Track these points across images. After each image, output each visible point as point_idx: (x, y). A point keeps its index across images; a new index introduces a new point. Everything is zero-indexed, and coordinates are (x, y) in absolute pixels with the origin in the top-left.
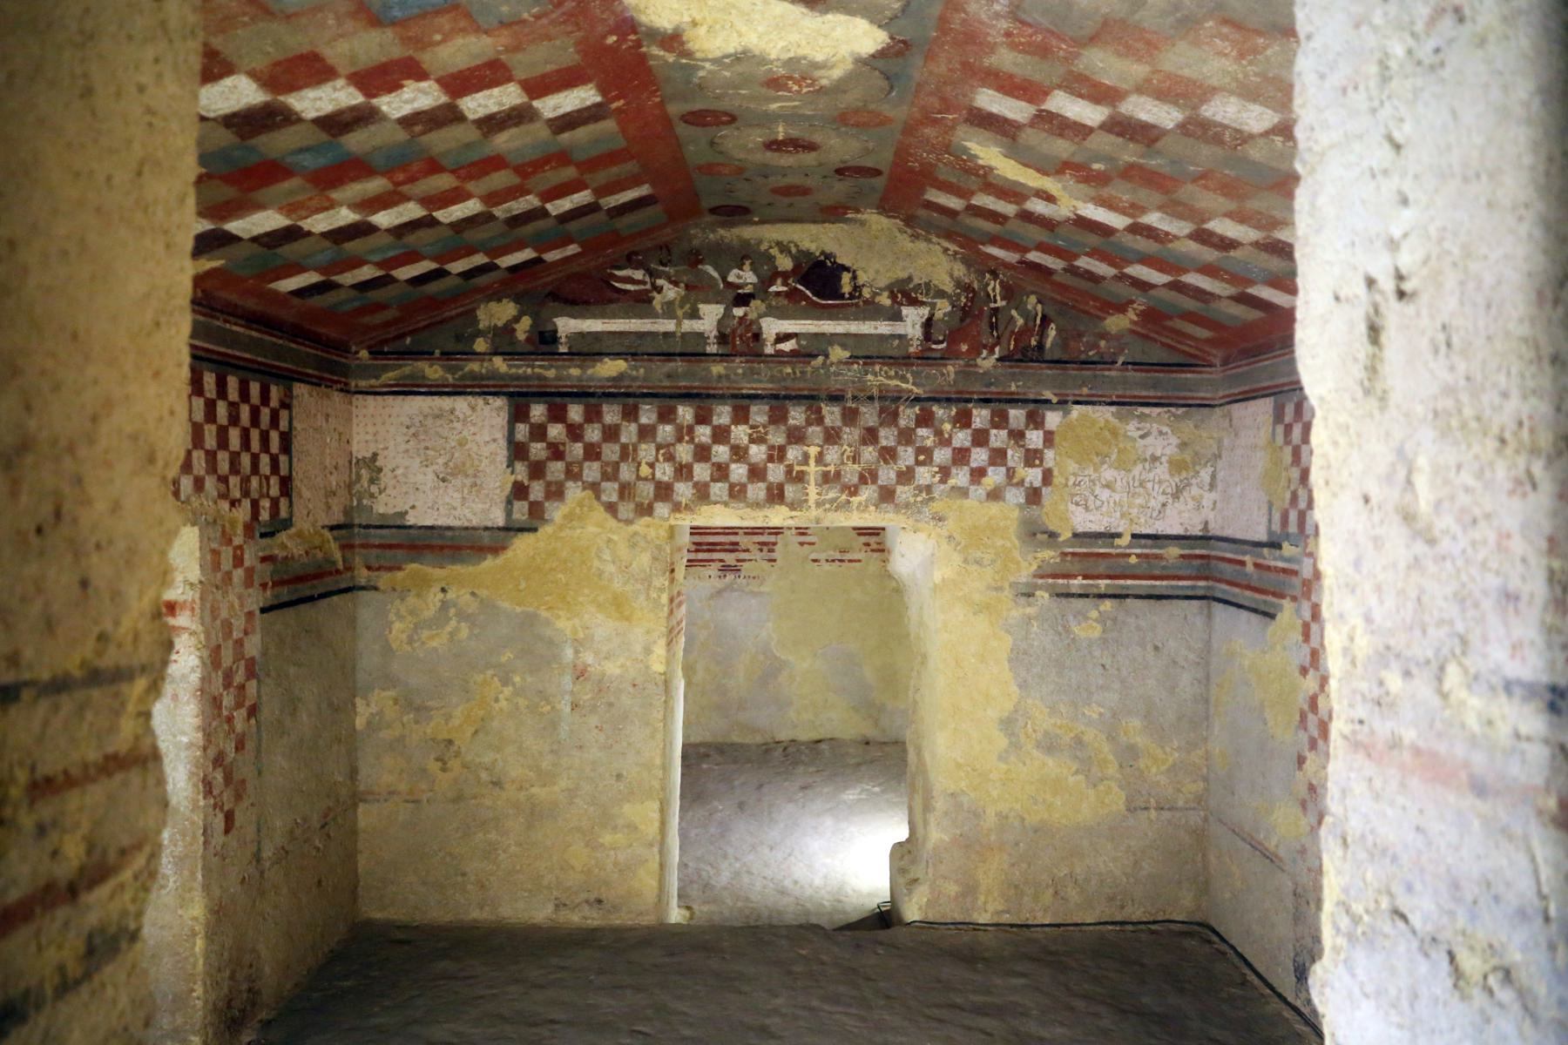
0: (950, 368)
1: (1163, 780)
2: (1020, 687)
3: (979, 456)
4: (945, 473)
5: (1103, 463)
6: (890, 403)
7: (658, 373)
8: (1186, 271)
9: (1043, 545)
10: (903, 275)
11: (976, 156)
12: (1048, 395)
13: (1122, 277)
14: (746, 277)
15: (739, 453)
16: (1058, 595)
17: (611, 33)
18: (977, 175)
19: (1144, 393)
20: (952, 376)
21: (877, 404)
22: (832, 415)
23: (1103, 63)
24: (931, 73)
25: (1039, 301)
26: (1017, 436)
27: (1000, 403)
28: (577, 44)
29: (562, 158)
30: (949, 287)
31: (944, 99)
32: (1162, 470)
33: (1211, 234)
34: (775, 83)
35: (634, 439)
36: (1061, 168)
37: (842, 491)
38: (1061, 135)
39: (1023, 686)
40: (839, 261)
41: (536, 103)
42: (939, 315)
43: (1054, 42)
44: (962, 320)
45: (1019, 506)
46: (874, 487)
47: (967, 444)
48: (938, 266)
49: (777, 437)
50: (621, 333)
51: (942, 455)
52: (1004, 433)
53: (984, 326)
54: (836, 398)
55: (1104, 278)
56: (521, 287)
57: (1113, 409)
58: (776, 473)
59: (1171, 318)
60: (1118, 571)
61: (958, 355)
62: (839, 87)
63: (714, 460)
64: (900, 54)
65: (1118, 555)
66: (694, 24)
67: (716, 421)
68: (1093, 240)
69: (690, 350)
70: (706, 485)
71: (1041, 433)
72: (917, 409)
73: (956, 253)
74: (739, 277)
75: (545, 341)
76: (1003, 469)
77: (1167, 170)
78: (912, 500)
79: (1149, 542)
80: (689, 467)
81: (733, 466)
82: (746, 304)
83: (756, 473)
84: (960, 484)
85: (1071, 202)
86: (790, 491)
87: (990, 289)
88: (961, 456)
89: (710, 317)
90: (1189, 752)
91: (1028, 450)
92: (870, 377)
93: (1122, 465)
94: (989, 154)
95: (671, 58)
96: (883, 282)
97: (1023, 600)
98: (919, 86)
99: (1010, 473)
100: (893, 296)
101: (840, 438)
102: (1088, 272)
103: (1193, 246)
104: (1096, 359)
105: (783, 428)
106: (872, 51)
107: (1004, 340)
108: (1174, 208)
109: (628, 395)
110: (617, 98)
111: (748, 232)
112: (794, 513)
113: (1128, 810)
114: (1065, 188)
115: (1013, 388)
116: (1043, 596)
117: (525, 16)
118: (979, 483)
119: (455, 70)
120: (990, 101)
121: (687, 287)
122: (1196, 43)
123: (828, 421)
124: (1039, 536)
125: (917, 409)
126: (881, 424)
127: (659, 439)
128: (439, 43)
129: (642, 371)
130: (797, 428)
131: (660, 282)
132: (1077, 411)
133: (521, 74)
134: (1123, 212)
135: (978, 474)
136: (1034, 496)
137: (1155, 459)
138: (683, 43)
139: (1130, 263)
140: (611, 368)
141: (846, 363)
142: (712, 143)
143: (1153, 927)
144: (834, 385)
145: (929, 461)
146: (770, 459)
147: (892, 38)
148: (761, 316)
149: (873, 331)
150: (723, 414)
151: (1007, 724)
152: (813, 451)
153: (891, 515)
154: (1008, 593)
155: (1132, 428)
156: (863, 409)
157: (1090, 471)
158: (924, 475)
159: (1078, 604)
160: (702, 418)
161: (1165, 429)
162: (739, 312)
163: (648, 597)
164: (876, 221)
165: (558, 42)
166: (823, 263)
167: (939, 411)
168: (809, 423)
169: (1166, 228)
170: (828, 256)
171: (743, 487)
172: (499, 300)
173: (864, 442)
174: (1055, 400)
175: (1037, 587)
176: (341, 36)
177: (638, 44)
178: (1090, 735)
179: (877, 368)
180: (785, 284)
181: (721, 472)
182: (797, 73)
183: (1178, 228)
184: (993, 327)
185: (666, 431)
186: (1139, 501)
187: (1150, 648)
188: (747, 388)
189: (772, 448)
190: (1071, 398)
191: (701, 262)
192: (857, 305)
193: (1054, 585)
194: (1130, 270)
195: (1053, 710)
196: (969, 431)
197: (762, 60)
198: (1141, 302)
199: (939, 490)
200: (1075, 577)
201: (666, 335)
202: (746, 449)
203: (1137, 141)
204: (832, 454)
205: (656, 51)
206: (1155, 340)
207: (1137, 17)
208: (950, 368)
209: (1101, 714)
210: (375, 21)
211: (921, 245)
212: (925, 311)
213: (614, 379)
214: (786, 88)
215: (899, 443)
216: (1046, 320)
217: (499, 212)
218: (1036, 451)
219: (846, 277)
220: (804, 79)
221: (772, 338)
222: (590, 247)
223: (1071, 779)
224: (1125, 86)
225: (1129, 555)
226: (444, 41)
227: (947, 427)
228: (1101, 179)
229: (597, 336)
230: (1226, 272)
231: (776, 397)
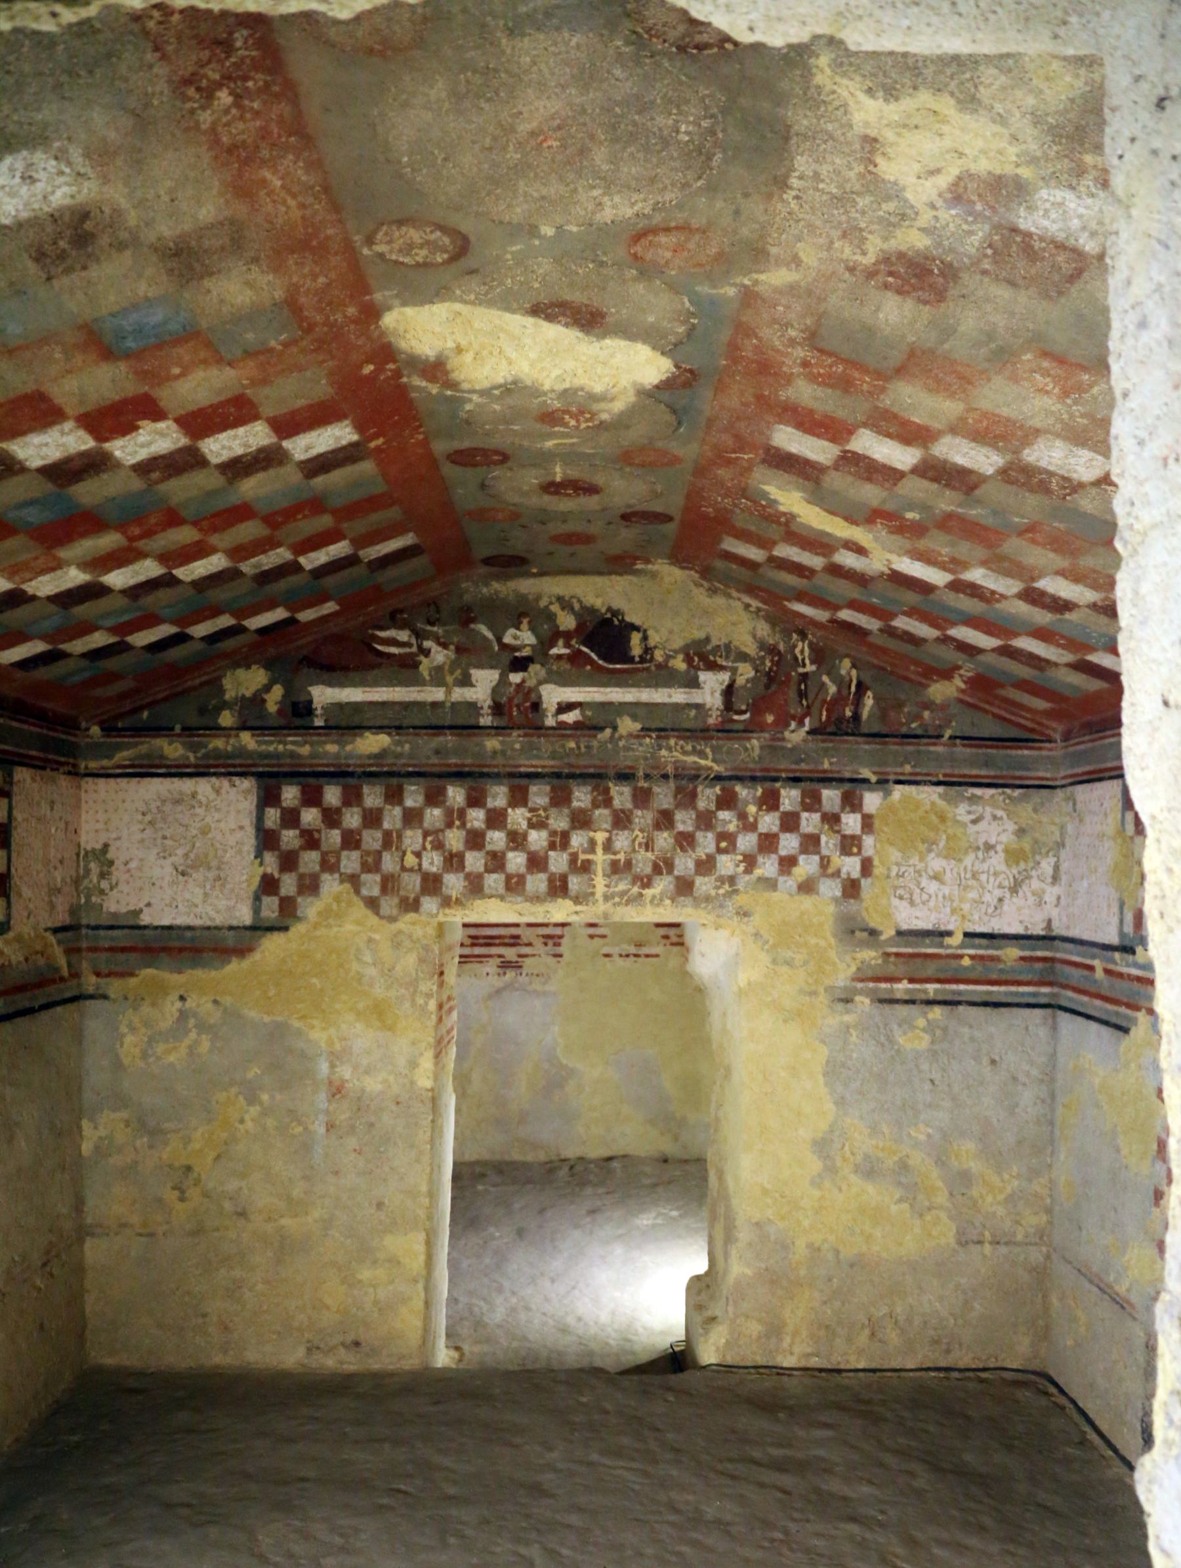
0: (755, 742)
1: (1001, 1211)
2: (836, 1103)
3: (789, 843)
4: (750, 862)
5: (930, 851)
6: (687, 783)
7: (425, 749)
8: (1016, 635)
9: (863, 944)
11: (775, 501)
12: (866, 773)
13: (946, 640)
14: (523, 638)
15: (517, 840)
16: (882, 1001)
17: (368, 362)
18: (779, 523)
19: (974, 772)
20: (757, 751)
21: (672, 784)
22: (621, 795)
23: (913, 399)
24: (722, 407)
25: (854, 666)
26: (832, 820)
27: (810, 782)
28: (331, 374)
29: (316, 505)
30: (751, 649)
31: (737, 437)
32: (997, 861)
33: (1043, 593)
34: (550, 418)
36: (872, 517)
37: (634, 883)
38: (869, 479)
39: (841, 1102)
40: (628, 619)
41: (286, 444)
42: (740, 681)
43: (857, 375)
44: (767, 687)
45: (835, 900)
46: (670, 878)
47: (775, 829)
49: (559, 822)
50: (383, 704)
51: (747, 842)
52: (816, 817)
53: (792, 694)
54: (625, 777)
55: (924, 640)
56: (272, 651)
57: (940, 789)
58: (558, 862)
59: (1002, 686)
60: (949, 975)
61: (762, 728)
62: (621, 422)
63: (489, 847)
64: (687, 385)
65: (948, 956)
66: (459, 350)
67: (490, 803)
68: (912, 598)
69: (460, 722)
70: (480, 877)
71: (858, 816)
72: (718, 789)
74: (516, 637)
75: (298, 713)
76: (816, 858)
77: (990, 521)
78: (713, 893)
79: (984, 942)
80: (460, 857)
81: (510, 855)
82: (524, 668)
83: (536, 862)
84: (767, 875)
85: (884, 555)
86: (574, 882)
87: (797, 651)
88: (768, 843)
89: (483, 684)
90: (1030, 1180)
91: (844, 837)
92: (664, 752)
93: (951, 853)
94: (790, 499)
95: (434, 389)
96: (678, 643)
97: (840, 1007)
98: (710, 422)
99: (825, 863)
100: (688, 660)
101: (630, 821)
102: (906, 633)
103: (1022, 608)
104: (919, 732)
106: (656, 382)
107: (814, 710)
108: (999, 564)
110: (376, 436)
112: (579, 908)
113: (959, 1243)
114: (876, 539)
115: (826, 766)
116: (863, 1002)
117: (273, 343)
118: (789, 873)
119: (194, 407)
120: (788, 439)
121: (459, 650)
122: (1015, 379)
123: (617, 803)
124: (858, 934)
126: (678, 806)
127: (427, 824)
128: (177, 377)
129: (407, 746)
130: (582, 811)
131: (427, 644)
132: (898, 792)
133: (268, 410)
134: (943, 567)
135: (788, 863)
136: (852, 889)
137: (989, 847)
138: (447, 373)
139: (954, 624)
140: (372, 743)
141: (637, 737)
142: (483, 486)
143: (984, 1375)
144: (624, 761)
145: (731, 849)
146: (552, 846)
147: (677, 366)
148: (540, 683)
149: (667, 700)
150: (498, 796)
151: (821, 1146)
152: (600, 837)
153: (689, 910)
154: (823, 998)
155: (962, 812)
156: (656, 789)
157: (915, 860)
158: (727, 864)
159: (903, 1011)
160: (475, 800)
161: (1000, 813)
162: (515, 678)
163: (413, 1001)
165: (308, 374)
166: (609, 621)
167: (742, 791)
168: (595, 805)
169: (992, 586)
170: (615, 613)
171: (521, 879)
172: (248, 667)
173: (658, 826)
174: (874, 779)
175: (856, 992)
176: (70, 372)
177: (398, 374)
178: (917, 1159)
179: (672, 742)
180: (567, 645)
181: (496, 862)
182: (575, 406)
183: (1007, 586)
184: (802, 695)
186: (972, 895)
187: (985, 1061)
188: (527, 764)
189: (553, 833)
190: (892, 777)
191: (473, 620)
192: (648, 669)
193: (875, 991)
194: (953, 632)
195: (874, 1130)
196: (777, 814)
197: (535, 391)
198: (968, 670)
199: (743, 881)
200: (899, 980)
201: (435, 705)
202: (525, 836)
203: (954, 488)
204: (622, 841)
205: (418, 382)
206: (986, 712)
207: (946, 346)
208: (755, 742)
209: (929, 1136)
210: (108, 354)
212: (725, 677)
214: (566, 425)
215: (698, 828)
216: (861, 688)
217: (247, 567)
218: (853, 837)
220: (582, 412)
221: (553, 708)
222: (349, 605)
223: (894, 1208)
224: (936, 425)
225: (961, 957)
226: (183, 375)
227: (752, 809)
228: (917, 530)
229: (356, 707)
230: (1063, 637)
231: (558, 775)
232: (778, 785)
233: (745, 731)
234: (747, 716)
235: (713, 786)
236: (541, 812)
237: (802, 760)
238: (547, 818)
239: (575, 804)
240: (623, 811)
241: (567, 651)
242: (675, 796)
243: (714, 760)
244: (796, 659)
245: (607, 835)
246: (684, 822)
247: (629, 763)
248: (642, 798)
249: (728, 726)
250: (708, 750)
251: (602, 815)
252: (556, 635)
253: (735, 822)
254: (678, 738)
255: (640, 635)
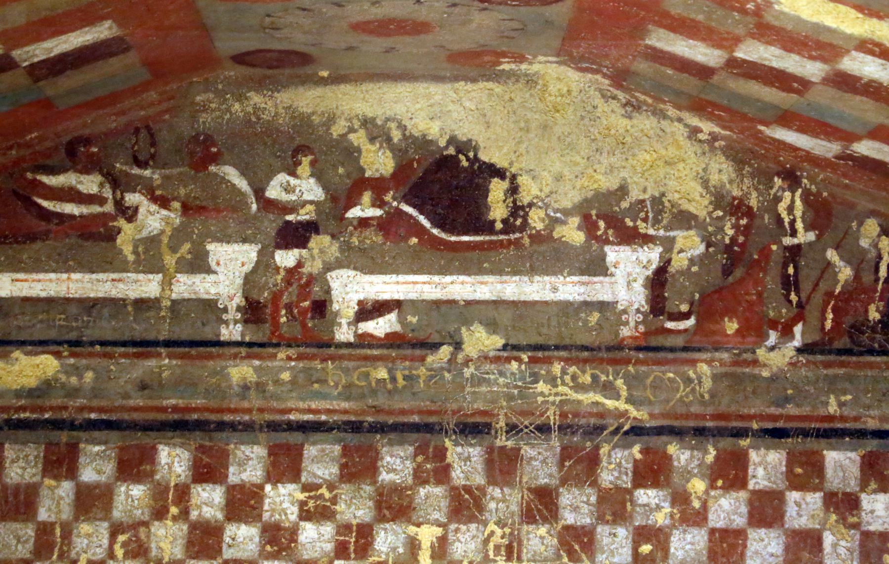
0: (704, 368)
10: (608, 183)
20: (708, 384)
21: (555, 442)
22: (466, 461)
30: (699, 205)
35: (66, 514)
40: (484, 157)
42: (679, 262)
44: (727, 271)
48: (677, 164)
53: (771, 282)
54: (473, 429)
67: (234, 476)
72: (636, 451)
73: (714, 138)
74: (288, 189)
82: (302, 243)
87: (782, 208)
89: (229, 269)
92: (541, 387)
96: (570, 197)
100: (588, 225)
101: (481, 508)
105: (368, 489)
107: (812, 312)
109: (57, 425)
111: (307, 100)
121: (186, 208)
123: (458, 475)
125: (636, 451)
126: (564, 482)
127: (116, 514)
129: (89, 376)
130: (397, 489)
141: (497, 359)
144: (472, 402)
148: (329, 267)
149: (549, 296)
150: (249, 463)
152: (427, 535)
156: (528, 451)
160: (207, 471)
162: (286, 258)
164: (558, 77)
166: (454, 159)
167: (680, 455)
168: (420, 478)
170: (463, 147)
173: (529, 516)
179: (557, 368)
180: (378, 202)
184: (789, 284)
185: (132, 496)
189: (344, 529)
191: (215, 159)
192: (517, 243)
201: (142, 304)
202: (294, 532)
211: (646, 123)
212: (652, 255)
213: (31, 393)
215: (601, 519)
219: (497, 189)
221: (350, 312)
227: (698, 486)
231: (355, 427)
232: (744, 443)
233: (685, 349)
234: (691, 322)
235: (629, 446)
236: (324, 491)
237: (787, 399)
238: (334, 500)
239: (385, 477)
240: (468, 489)
241: (378, 212)
242: (561, 464)
243: (629, 401)
244: (779, 220)
245: (439, 531)
246: (575, 509)
247: (480, 405)
248: (503, 466)
249: (654, 342)
250: (619, 382)
251: (432, 496)
252: (361, 184)
253: (667, 509)
254: (567, 360)
255: (506, 184)
